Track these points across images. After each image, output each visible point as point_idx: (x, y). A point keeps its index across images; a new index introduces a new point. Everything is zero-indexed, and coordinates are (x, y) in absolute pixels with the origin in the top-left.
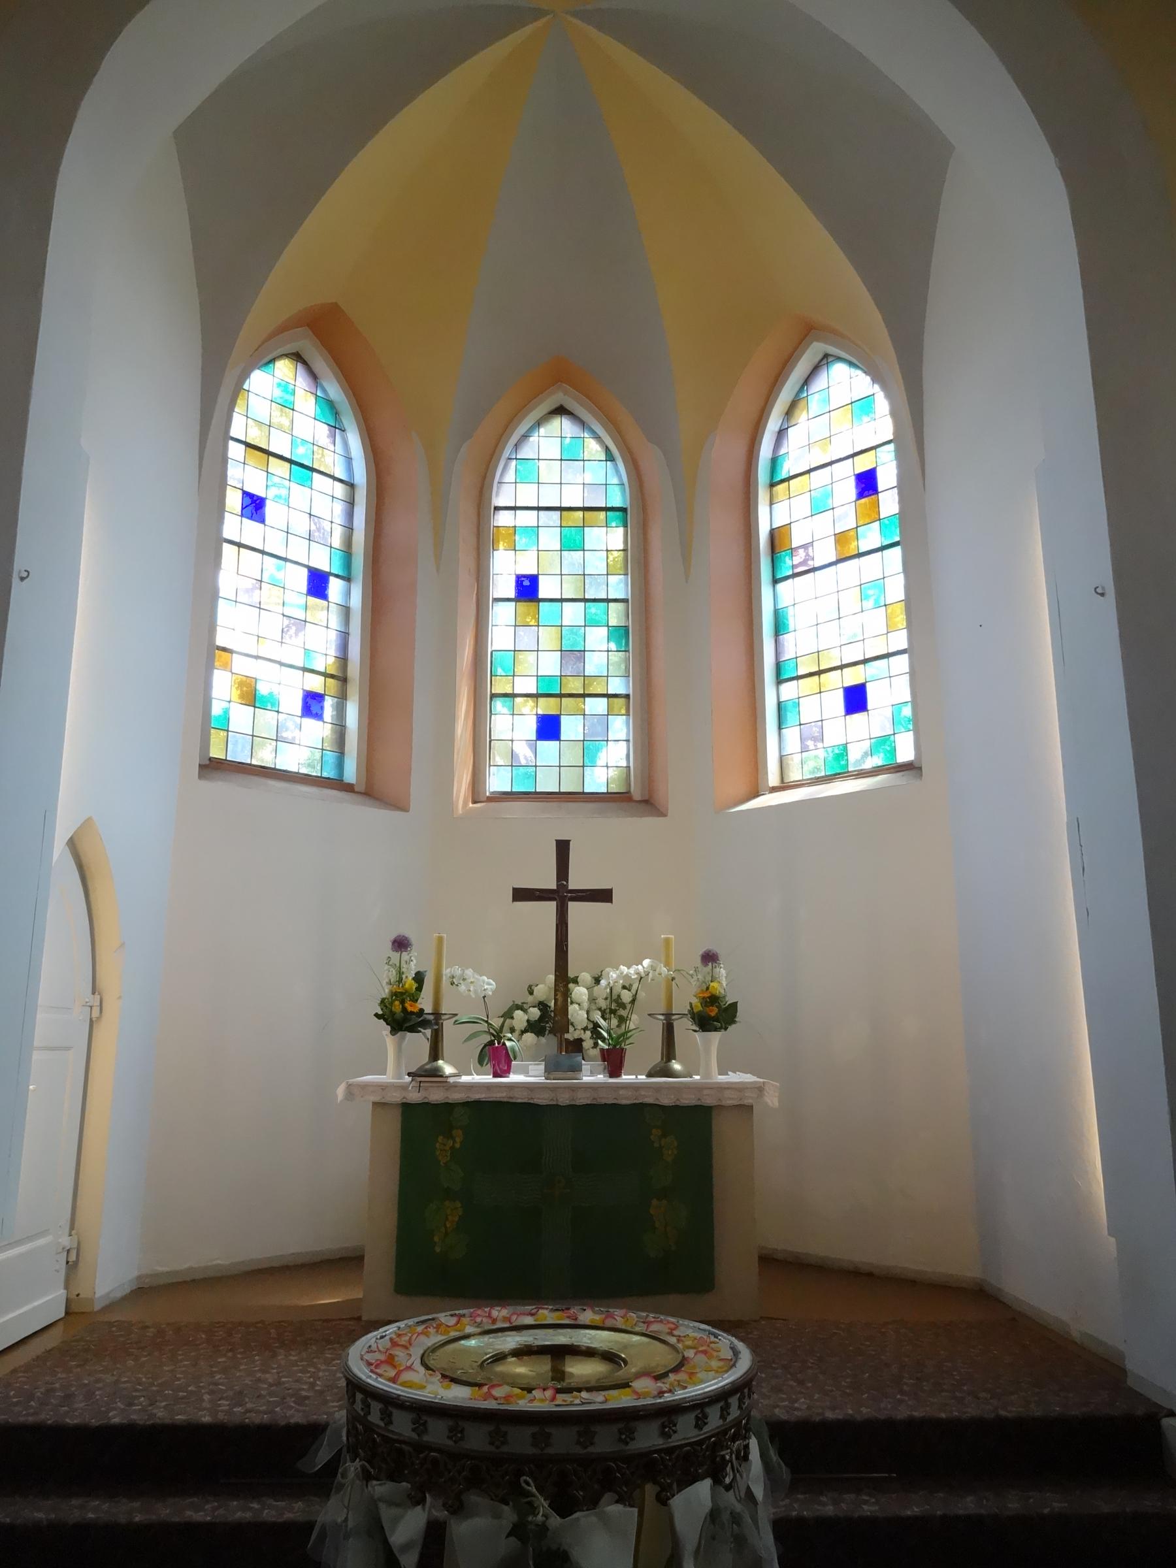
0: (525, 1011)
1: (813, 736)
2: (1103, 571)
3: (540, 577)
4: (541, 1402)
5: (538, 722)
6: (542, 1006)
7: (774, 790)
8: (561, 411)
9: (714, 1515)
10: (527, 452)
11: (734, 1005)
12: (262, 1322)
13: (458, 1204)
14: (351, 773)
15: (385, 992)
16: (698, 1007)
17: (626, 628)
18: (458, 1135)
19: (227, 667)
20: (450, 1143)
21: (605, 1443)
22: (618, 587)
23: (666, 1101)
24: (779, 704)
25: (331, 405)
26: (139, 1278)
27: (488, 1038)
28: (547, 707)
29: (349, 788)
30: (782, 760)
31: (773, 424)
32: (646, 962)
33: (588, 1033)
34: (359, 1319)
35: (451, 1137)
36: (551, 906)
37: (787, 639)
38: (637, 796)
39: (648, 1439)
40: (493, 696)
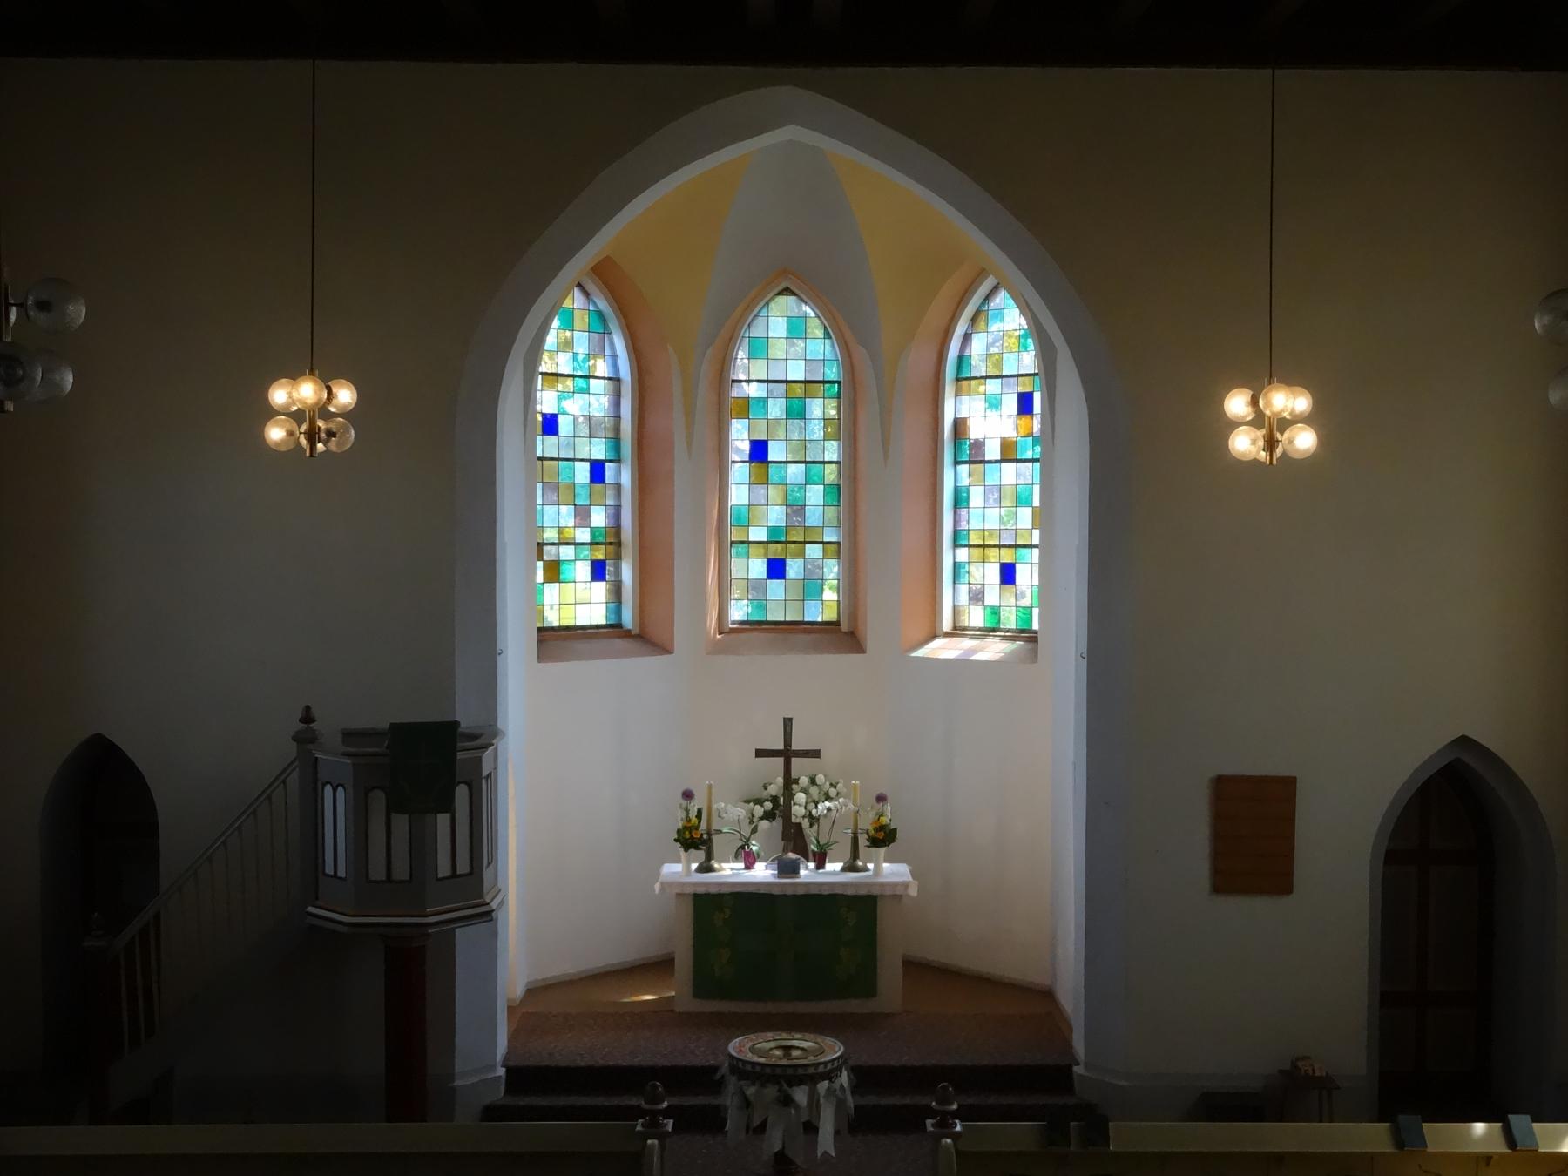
0: (762, 806)
1: (977, 597)
2: (1084, 649)
3: (769, 442)
4: (785, 1062)
5: (771, 579)
6: (774, 799)
7: (947, 635)
8: (787, 291)
9: (829, 1089)
10: (757, 331)
11: (895, 830)
14: (628, 619)
15: (680, 825)
16: (872, 832)
17: (839, 486)
18: (727, 911)
19: (540, 557)
21: (800, 1071)
22: (832, 451)
23: (850, 892)
24: (955, 563)
25: (600, 314)
26: (529, 982)
27: (741, 843)
28: (776, 551)
29: (627, 634)
30: (955, 608)
31: (960, 330)
32: (841, 800)
33: (806, 820)
36: (781, 760)
37: (963, 512)
38: (844, 627)
39: (811, 1071)
40: (732, 542)
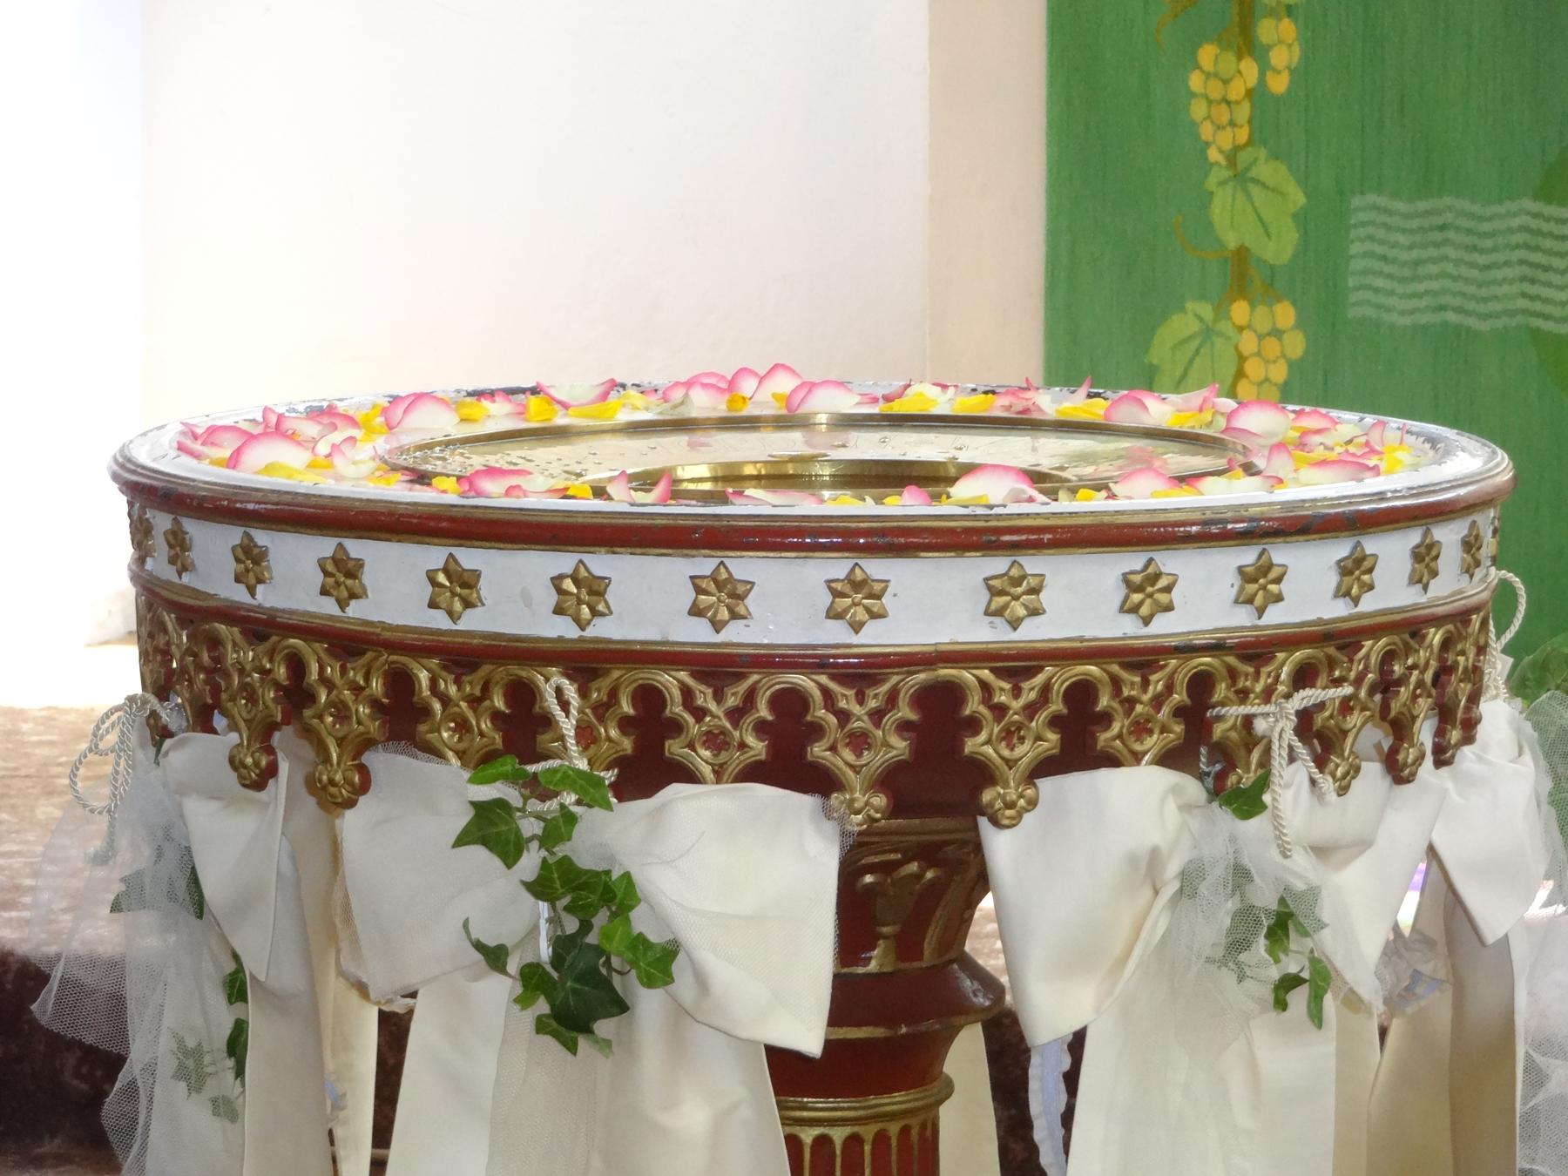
13: (1285, 314)
20: (1250, 69)
35: (1246, 43)
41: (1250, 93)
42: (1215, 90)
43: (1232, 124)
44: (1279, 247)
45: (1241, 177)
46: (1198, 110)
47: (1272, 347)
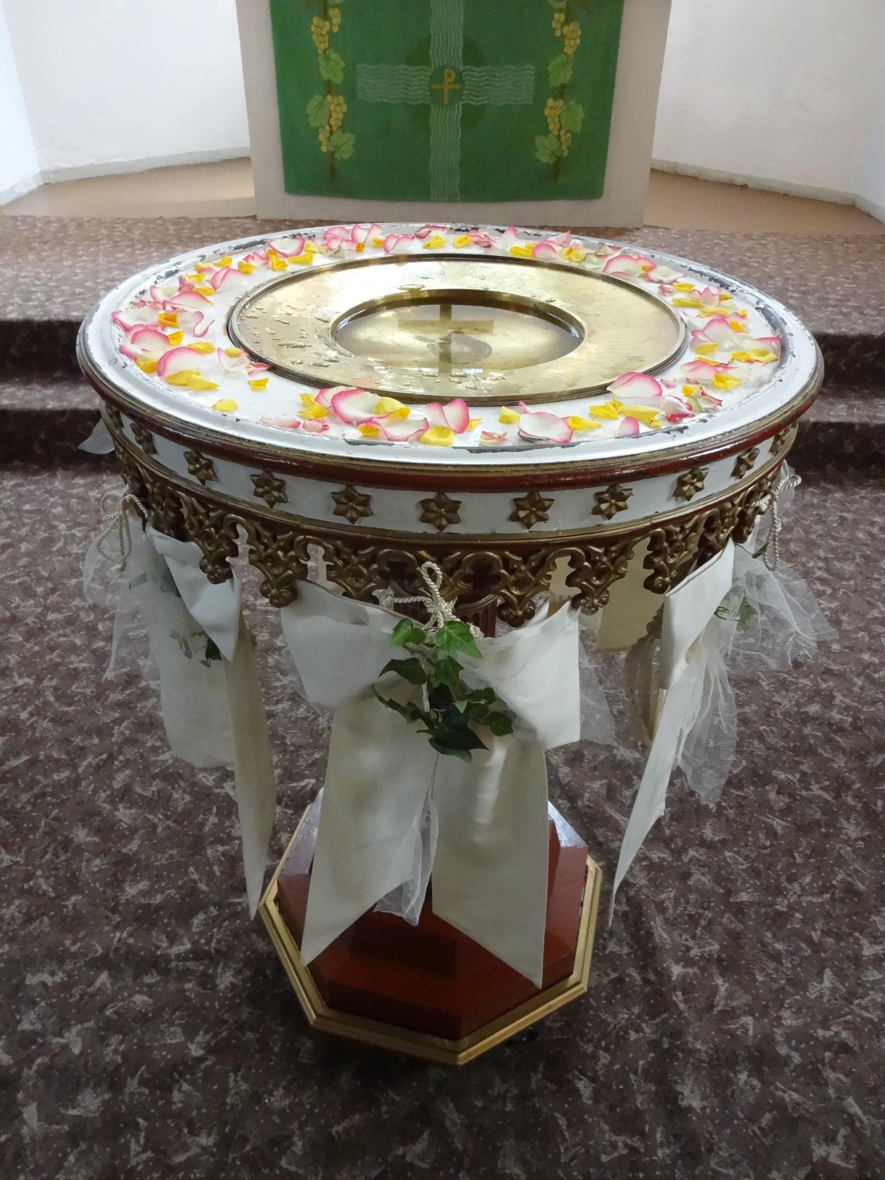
12: (161, 218)
13: (341, 99)
26: (43, 173)
34: (254, 217)
35: (326, 17)
41: (328, 32)
42: (319, 31)
43: (324, 42)
44: (338, 79)
45: (327, 58)
46: (315, 37)
47: (338, 108)
